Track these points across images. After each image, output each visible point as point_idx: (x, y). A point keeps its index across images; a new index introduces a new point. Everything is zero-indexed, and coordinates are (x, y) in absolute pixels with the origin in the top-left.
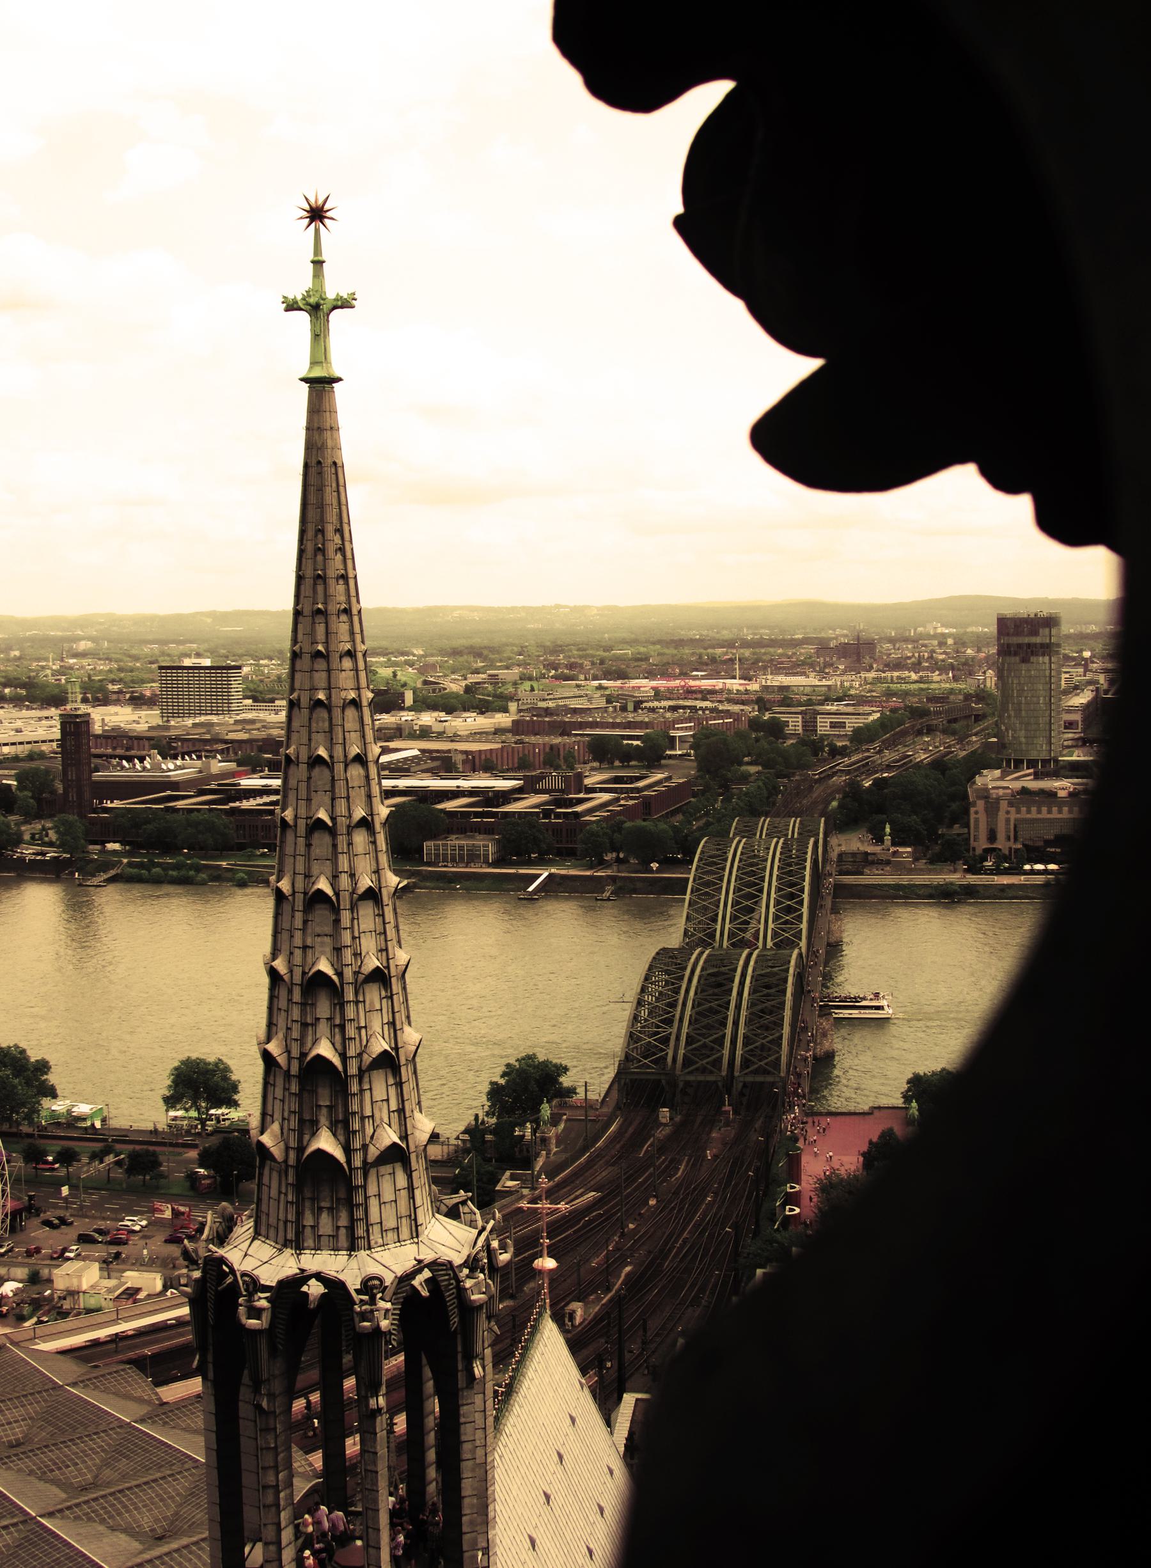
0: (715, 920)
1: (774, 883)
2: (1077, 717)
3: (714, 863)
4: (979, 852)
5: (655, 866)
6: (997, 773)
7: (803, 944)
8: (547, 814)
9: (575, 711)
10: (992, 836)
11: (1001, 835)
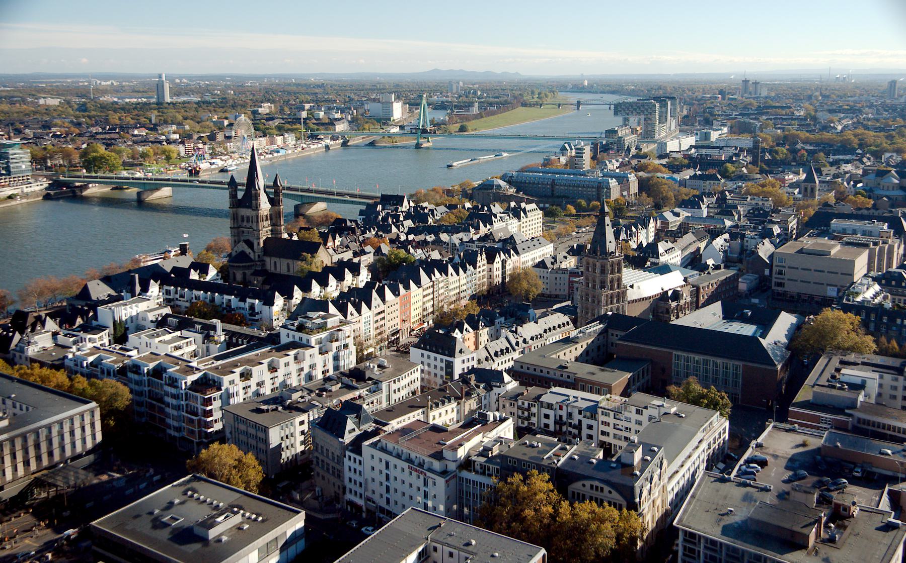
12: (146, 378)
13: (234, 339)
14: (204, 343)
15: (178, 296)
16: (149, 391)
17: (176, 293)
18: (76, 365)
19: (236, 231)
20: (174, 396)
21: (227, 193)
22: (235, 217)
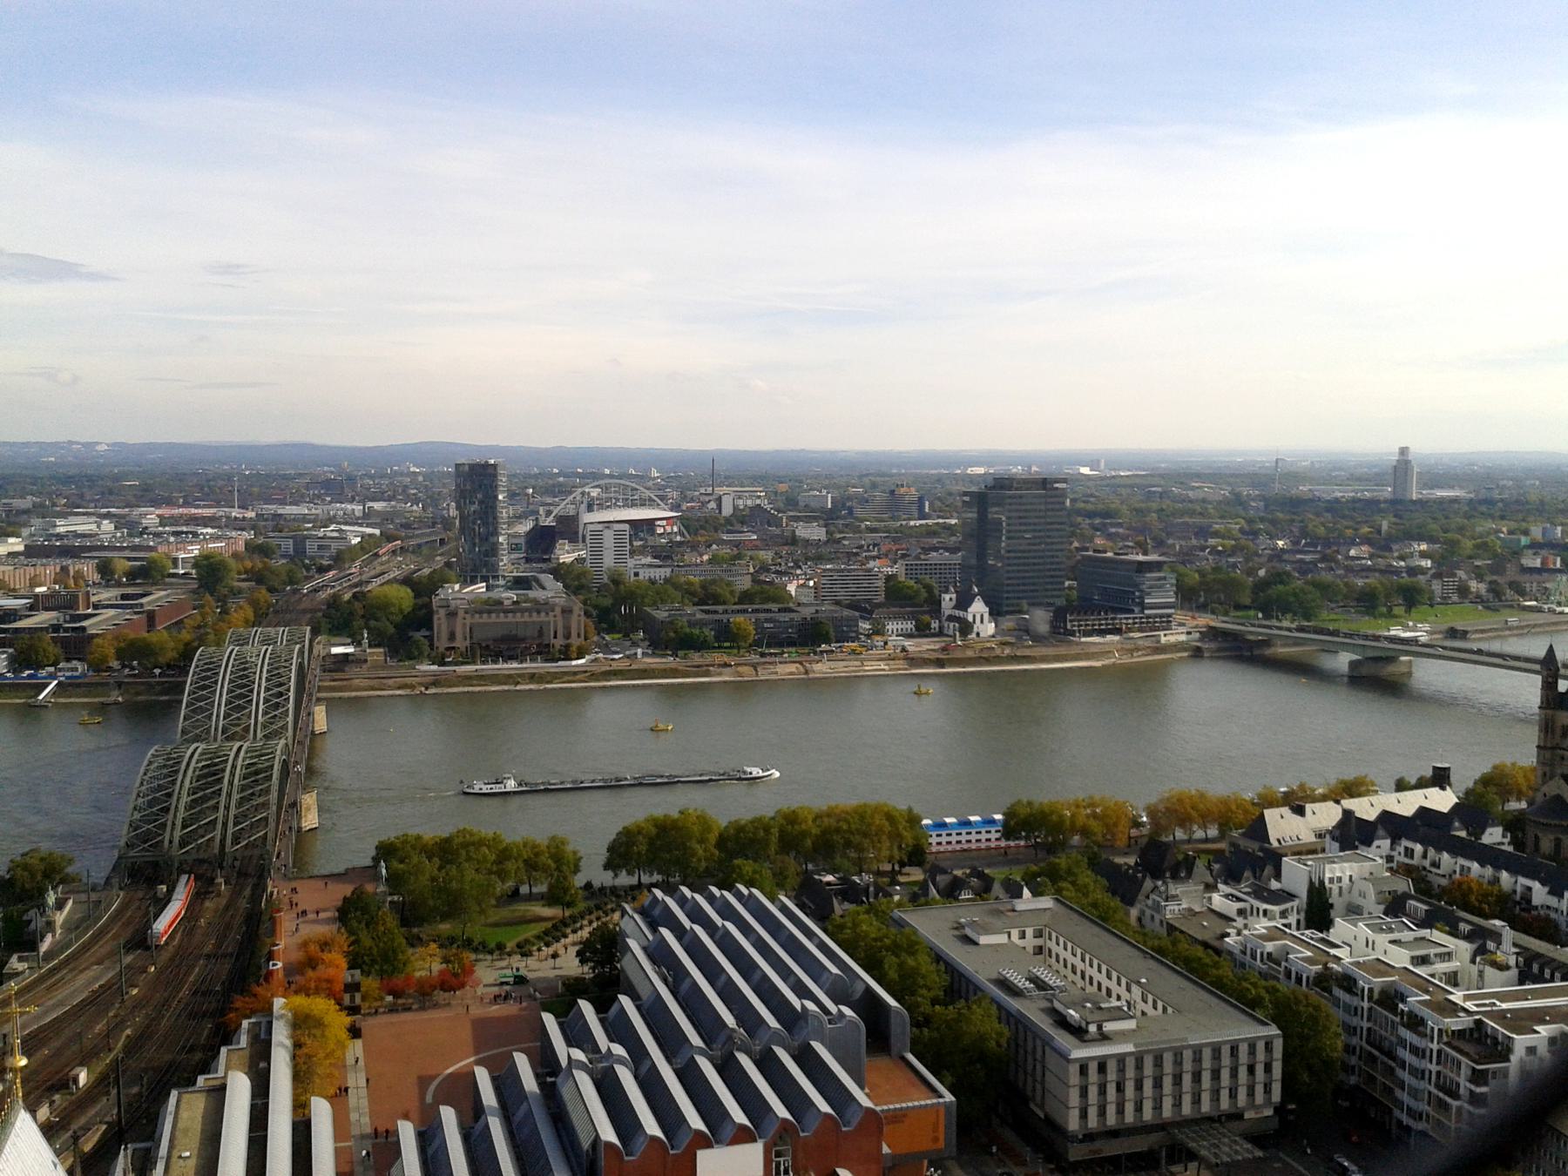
2: (522, 541)
3: (210, 670)
4: (441, 649)
5: (157, 671)
6: (457, 587)
7: (290, 733)
8: (56, 628)
9: (84, 536)
10: (452, 637)
11: (459, 635)
12: (1366, 1005)
13: (1535, 968)
14: (1473, 961)
15: (1427, 863)
16: (1369, 1029)
17: (1425, 856)
18: (1244, 953)
19: (1548, 754)
20: (1415, 1051)
21: (1537, 680)
22: (1547, 727)
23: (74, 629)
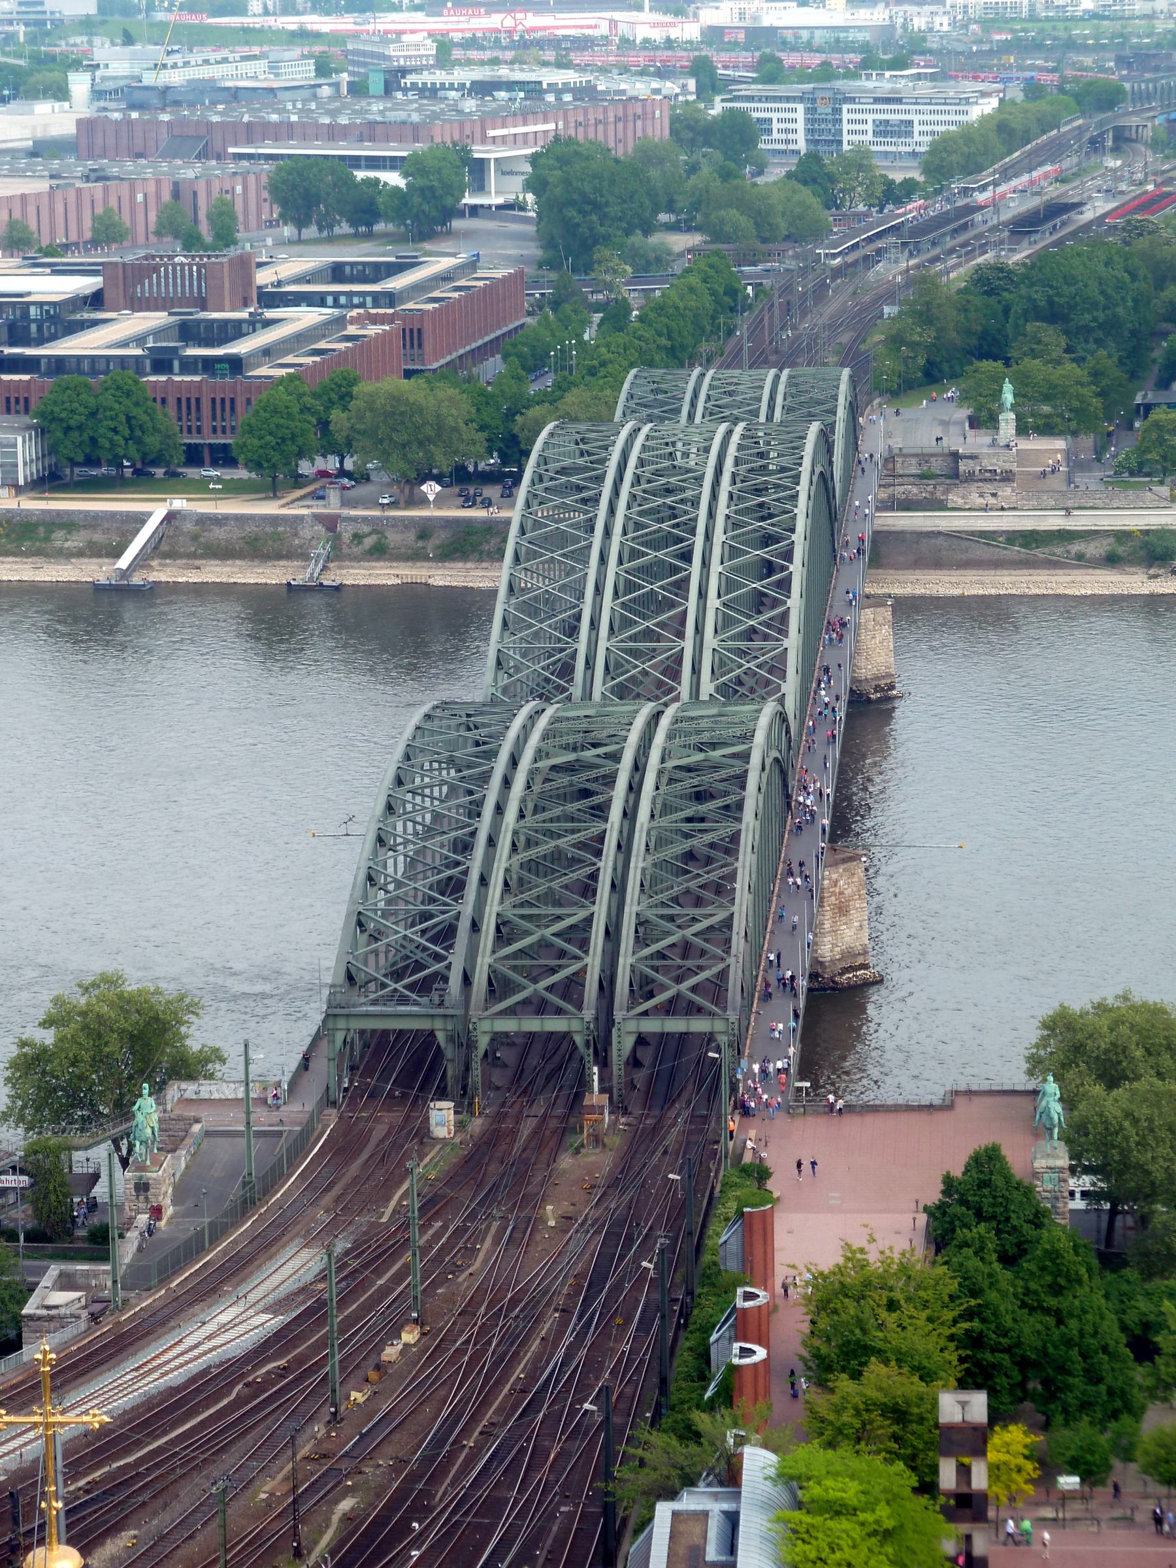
0: (572, 630)
1: (719, 537)
23: (208, 364)
